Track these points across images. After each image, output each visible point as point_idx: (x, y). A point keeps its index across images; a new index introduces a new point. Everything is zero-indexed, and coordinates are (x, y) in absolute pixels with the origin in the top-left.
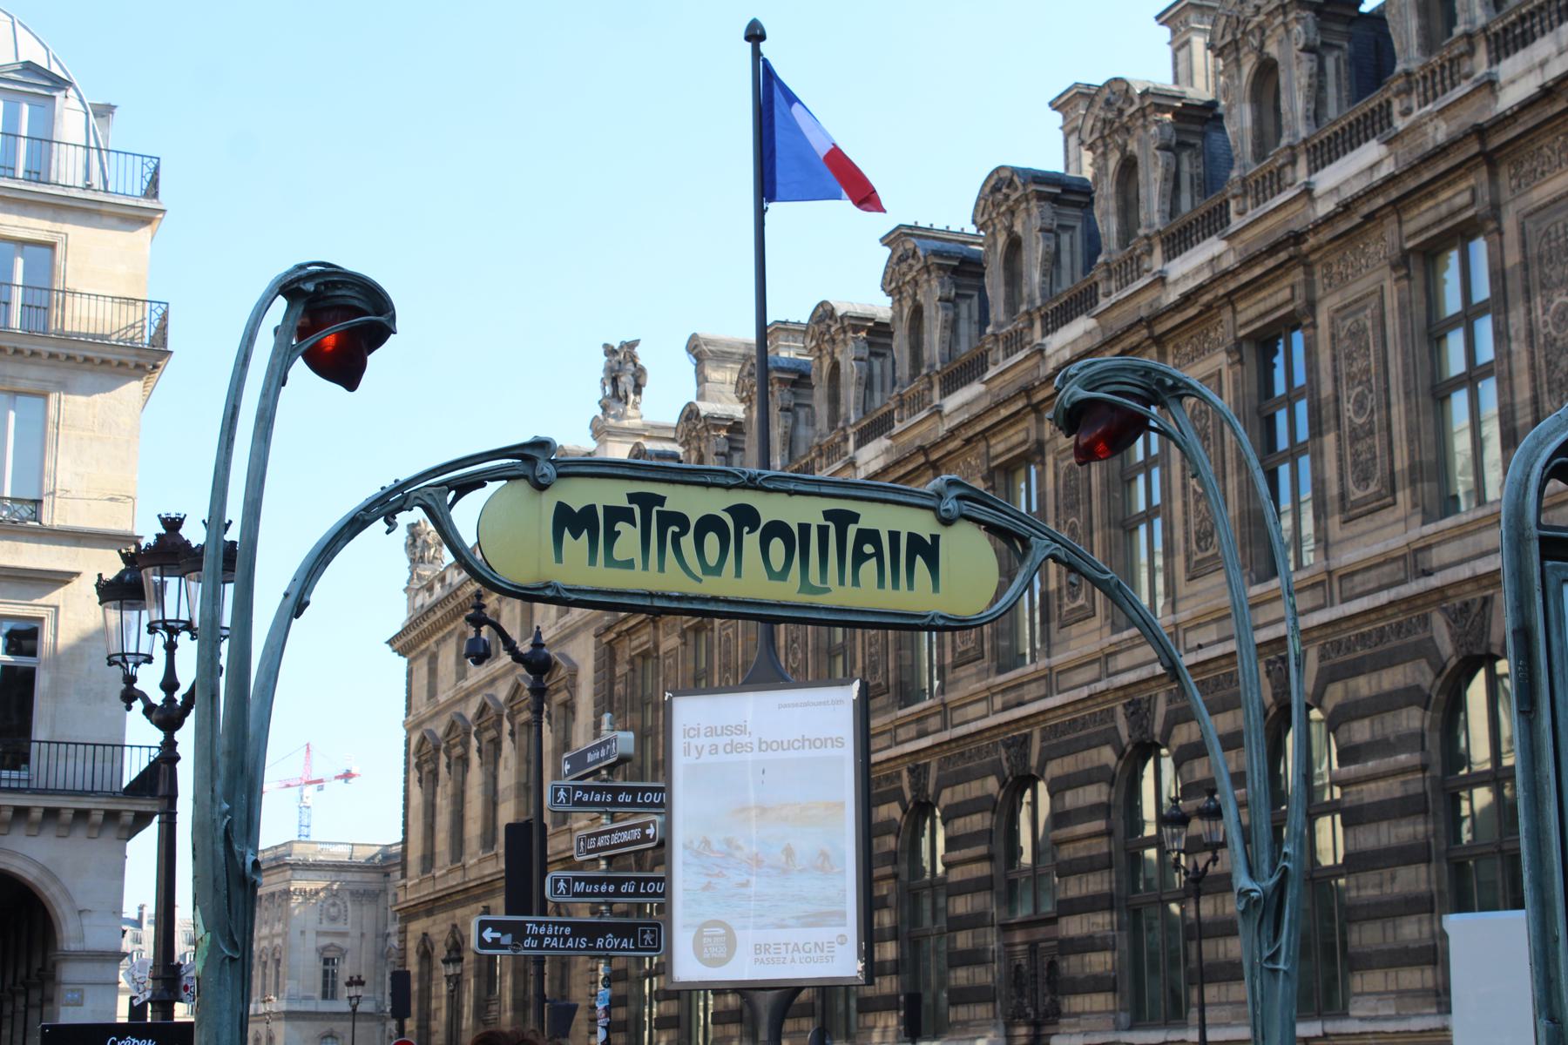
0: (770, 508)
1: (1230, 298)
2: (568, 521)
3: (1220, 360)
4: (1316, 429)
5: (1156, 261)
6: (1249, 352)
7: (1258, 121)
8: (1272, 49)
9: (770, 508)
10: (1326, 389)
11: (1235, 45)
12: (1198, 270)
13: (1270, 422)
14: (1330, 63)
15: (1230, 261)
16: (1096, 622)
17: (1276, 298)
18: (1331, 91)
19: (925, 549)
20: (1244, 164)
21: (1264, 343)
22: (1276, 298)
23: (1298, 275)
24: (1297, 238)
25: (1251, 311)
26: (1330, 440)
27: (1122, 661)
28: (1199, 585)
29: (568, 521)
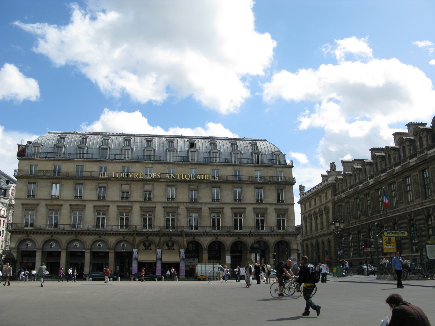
0: (397, 232)
1: (418, 166)
2: (388, 233)
3: (417, 173)
4: (430, 181)
5: (408, 160)
6: (421, 172)
7: (420, 144)
8: (421, 136)
9: (397, 232)
10: (431, 178)
11: (416, 135)
12: (414, 162)
13: (424, 181)
14: (429, 137)
15: (418, 161)
16: (404, 204)
17: (424, 166)
18: (429, 140)
19: (404, 233)
20: (419, 150)
21: (423, 171)
22: (424, 166)
23: (426, 164)
24: (426, 160)
25: (421, 168)
26: (432, 184)
27: (407, 209)
28: (417, 200)
29: (388, 233)
